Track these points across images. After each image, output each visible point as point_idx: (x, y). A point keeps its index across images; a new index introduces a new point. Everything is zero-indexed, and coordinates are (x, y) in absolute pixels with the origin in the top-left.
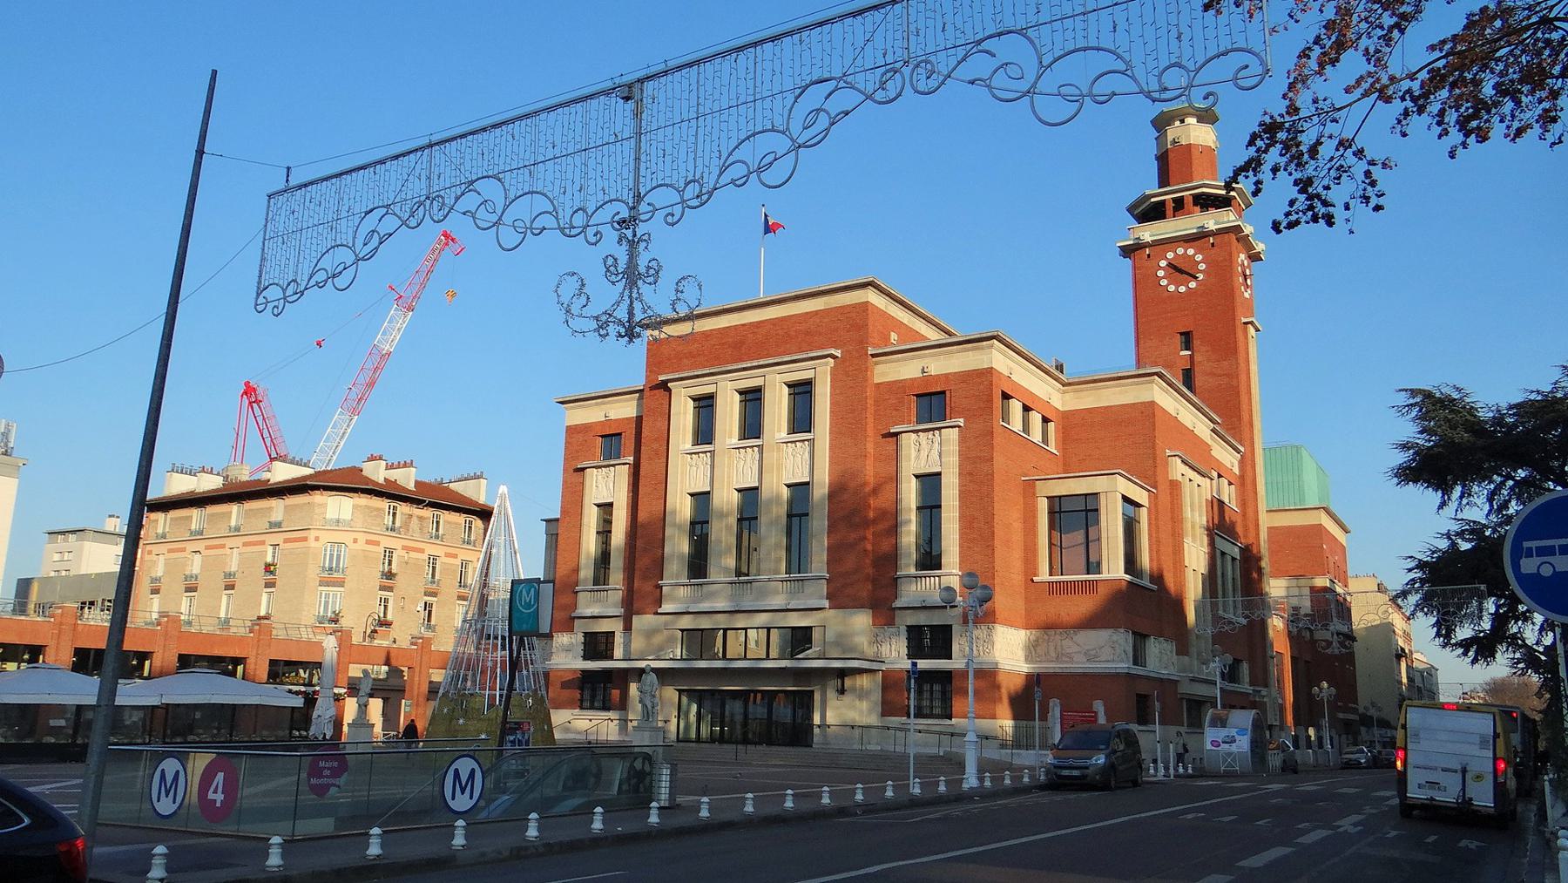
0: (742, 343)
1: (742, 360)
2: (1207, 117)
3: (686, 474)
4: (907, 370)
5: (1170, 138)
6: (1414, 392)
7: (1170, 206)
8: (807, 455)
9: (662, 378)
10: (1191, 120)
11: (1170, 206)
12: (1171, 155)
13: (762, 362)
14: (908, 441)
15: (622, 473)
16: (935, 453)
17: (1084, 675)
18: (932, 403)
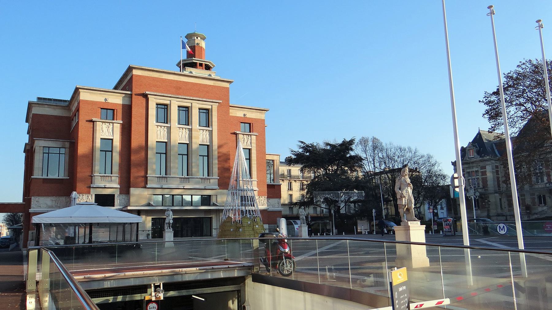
0: (180, 88)
1: (180, 95)
2: (203, 39)
3: (157, 133)
4: (239, 114)
5: (196, 42)
6: (302, 142)
7: (198, 65)
8: (208, 136)
9: (147, 93)
10: (199, 38)
11: (198, 65)
12: (196, 48)
13: (194, 98)
14: (241, 136)
15: (117, 127)
16: (249, 142)
17: (272, 211)
18: (250, 126)
